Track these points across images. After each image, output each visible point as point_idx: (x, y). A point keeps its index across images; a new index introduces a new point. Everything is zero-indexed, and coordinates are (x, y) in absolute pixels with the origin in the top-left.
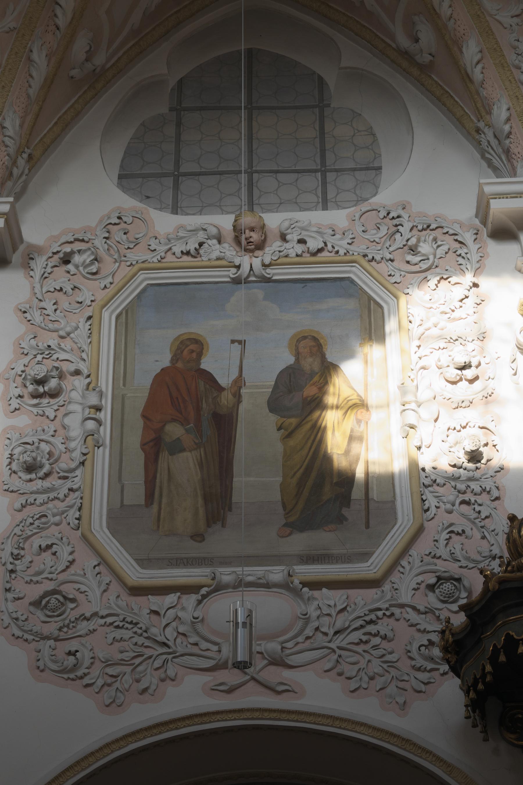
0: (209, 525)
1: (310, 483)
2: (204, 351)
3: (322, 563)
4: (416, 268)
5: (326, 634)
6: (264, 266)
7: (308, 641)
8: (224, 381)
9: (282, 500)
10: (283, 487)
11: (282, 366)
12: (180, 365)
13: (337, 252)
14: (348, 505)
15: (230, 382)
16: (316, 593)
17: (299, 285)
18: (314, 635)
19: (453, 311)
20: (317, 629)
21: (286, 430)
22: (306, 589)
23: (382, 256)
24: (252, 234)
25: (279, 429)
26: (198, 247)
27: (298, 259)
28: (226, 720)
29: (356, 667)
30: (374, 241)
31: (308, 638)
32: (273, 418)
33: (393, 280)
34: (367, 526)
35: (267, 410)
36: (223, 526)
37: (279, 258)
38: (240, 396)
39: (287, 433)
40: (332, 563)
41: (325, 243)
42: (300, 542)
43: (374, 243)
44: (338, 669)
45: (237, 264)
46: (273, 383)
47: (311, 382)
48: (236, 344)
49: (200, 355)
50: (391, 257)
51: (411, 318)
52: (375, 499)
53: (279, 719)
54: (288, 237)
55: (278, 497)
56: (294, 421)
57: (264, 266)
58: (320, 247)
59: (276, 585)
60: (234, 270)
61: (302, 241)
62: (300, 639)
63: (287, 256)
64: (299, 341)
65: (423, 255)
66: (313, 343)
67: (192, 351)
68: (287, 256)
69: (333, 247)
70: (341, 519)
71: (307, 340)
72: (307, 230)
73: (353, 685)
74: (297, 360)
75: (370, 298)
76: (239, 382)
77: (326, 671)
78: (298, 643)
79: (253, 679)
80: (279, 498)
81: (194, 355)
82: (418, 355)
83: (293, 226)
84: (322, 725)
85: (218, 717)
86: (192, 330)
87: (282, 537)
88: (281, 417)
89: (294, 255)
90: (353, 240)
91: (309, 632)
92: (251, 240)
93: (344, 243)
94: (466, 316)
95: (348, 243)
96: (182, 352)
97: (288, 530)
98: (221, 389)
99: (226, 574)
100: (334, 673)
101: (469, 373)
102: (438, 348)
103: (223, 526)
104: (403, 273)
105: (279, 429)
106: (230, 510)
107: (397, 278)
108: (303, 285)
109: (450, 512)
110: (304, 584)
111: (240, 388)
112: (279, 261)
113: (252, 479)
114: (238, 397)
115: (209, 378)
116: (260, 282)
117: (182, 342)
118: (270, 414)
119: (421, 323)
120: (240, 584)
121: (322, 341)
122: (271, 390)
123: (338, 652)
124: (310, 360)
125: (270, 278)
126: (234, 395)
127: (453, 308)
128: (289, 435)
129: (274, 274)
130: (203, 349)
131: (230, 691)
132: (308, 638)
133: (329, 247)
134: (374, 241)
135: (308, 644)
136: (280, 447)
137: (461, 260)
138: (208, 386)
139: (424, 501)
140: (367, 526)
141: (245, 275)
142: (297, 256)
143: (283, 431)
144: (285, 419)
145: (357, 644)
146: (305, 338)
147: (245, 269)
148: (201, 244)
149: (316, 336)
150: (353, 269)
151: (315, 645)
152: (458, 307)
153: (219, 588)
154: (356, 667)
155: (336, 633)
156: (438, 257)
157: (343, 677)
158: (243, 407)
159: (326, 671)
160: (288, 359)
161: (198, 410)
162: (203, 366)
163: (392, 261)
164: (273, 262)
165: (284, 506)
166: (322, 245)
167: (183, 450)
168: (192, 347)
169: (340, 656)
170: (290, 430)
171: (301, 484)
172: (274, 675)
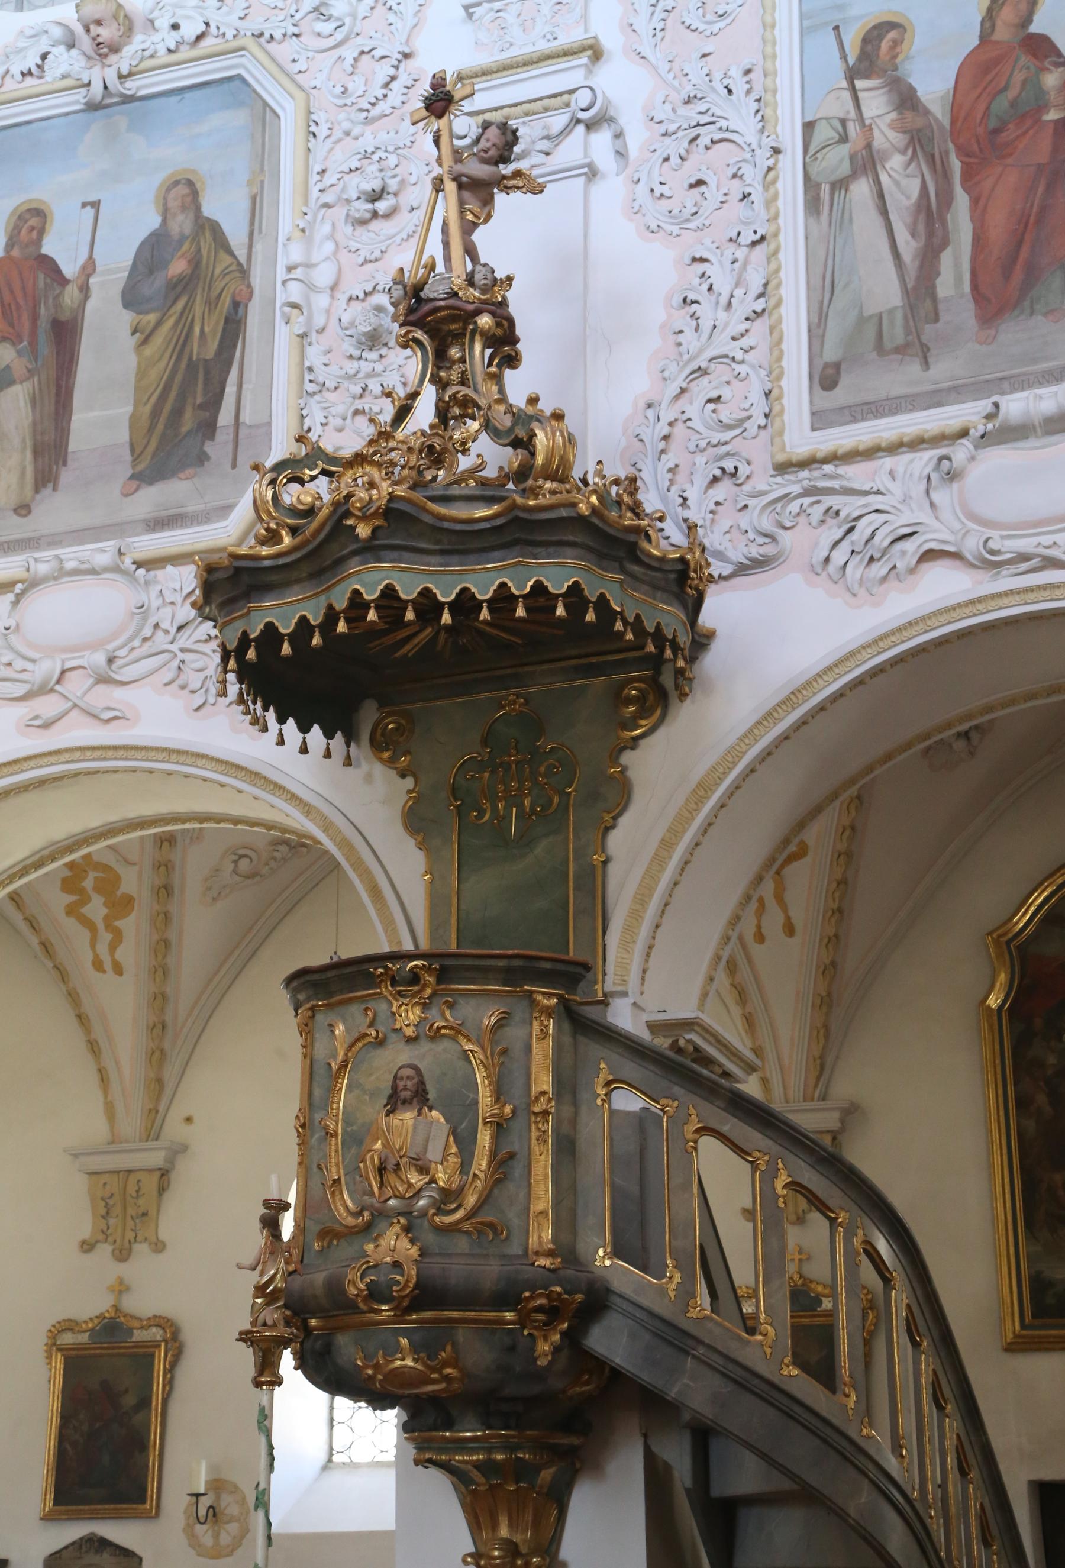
0: (37, 491)
1: (168, 407)
2: (47, 226)
3: (173, 529)
4: (331, 42)
5: (167, 632)
6: (121, 77)
7: (149, 643)
8: (69, 268)
9: (131, 439)
10: (133, 419)
11: (143, 234)
12: (16, 253)
13: (224, 34)
14: (212, 437)
15: (77, 269)
16: (160, 573)
17: (173, 99)
18: (153, 634)
19: (373, 104)
20: (156, 626)
21: (142, 333)
22: (141, 571)
23: (283, 31)
24: (100, 30)
25: (133, 333)
26: (40, 62)
27: (173, 58)
28: (41, 767)
29: (202, 675)
30: (276, 7)
31: (145, 640)
32: (127, 318)
33: (297, 67)
34: (234, 466)
35: (121, 306)
36: (55, 489)
37: (141, 61)
38: (88, 288)
39: (143, 337)
40: (186, 527)
41: (207, 24)
42: (151, 498)
43: (276, 11)
44: (179, 682)
45: (86, 82)
46: (130, 263)
47: (180, 253)
48: (88, 208)
49: (42, 232)
50: (296, 30)
51: (313, 128)
52: (247, 422)
53: (105, 759)
54: (157, 24)
55: (124, 436)
56: (152, 318)
57: (121, 77)
58: (199, 32)
59: (106, 570)
60: (83, 90)
61: (175, 27)
62: (136, 643)
63: (152, 56)
64: (168, 190)
65: (338, 19)
66: (186, 191)
67: (32, 229)
68: (152, 56)
69: (218, 28)
70: (202, 459)
71: (180, 186)
72: (181, 7)
73: (198, 699)
74: (164, 221)
75: (266, 104)
76: (89, 267)
77: (166, 685)
78: (133, 649)
79: (75, 706)
80: (127, 438)
81: (34, 234)
82: (320, 186)
83: (161, 5)
84: (156, 761)
85: (32, 763)
86: (33, 195)
87: (127, 495)
88: (139, 313)
89: (162, 51)
90: (247, 11)
91: (147, 632)
92: (100, 40)
93: (234, 17)
94: (391, 110)
95: (241, 18)
96: (19, 232)
97: (134, 484)
98: (64, 281)
99: (42, 562)
100: (174, 686)
101: (382, 206)
102: (348, 170)
103: (55, 489)
104: (310, 54)
105: (133, 333)
106: (65, 464)
107: (302, 65)
108: (179, 98)
109: (340, 430)
110: (139, 564)
111: (89, 276)
112: (142, 66)
113: (96, 413)
114: (85, 290)
115: (49, 265)
116: (123, 103)
117: (20, 217)
118: (125, 311)
119: (329, 132)
120: (61, 574)
121: (198, 185)
122: (126, 274)
123: (181, 656)
124: (181, 217)
125: (132, 96)
126: (81, 289)
127: (373, 100)
128: (145, 342)
129: (138, 89)
130: (45, 222)
131: (47, 725)
132: (145, 640)
133: (213, 29)
134: (276, 7)
135: (146, 648)
136: (132, 360)
137: (392, 18)
138: (48, 280)
139: (303, 417)
140: (234, 466)
141: (99, 98)
142: (170, 51)
143: (138, 334)
144: (141, 316)
145: (206, 641)
146: (177, 183)
147: (97, 89)
148: (44, 57)
149: (191, 178)
150: (243, 60)
151: (154, 650)
152: (380, 97)
153: (33, 583)
154: (202, 675)
155: (180, 628)
156: (360, 16)
157: (186, 691)
158: (90, 305)
159: (166, 685)
160: (153, 221)
161: (35, 318)
162: (46, 250)
163: (297, 36)
164: (134, 69)
165: (132, 450)
166: (203, 27)
167: (12, 383)
168: (33, 221)
169: (183, 662)
170: (147, 333)
171: (155, 413)
172: (102, 697)
